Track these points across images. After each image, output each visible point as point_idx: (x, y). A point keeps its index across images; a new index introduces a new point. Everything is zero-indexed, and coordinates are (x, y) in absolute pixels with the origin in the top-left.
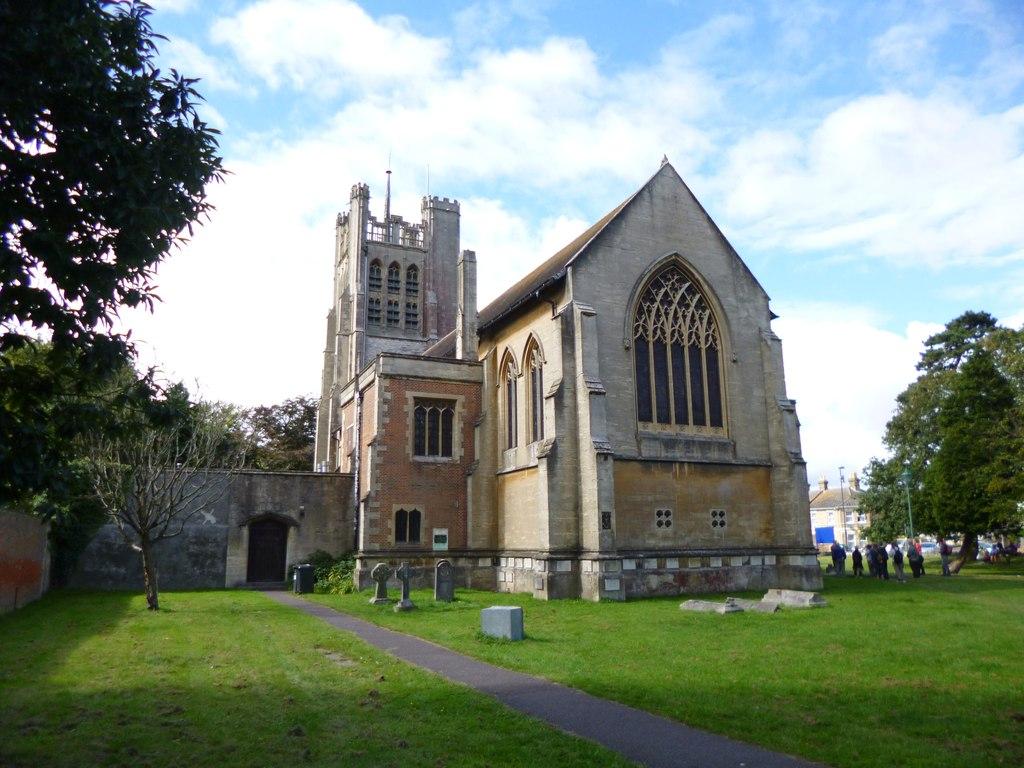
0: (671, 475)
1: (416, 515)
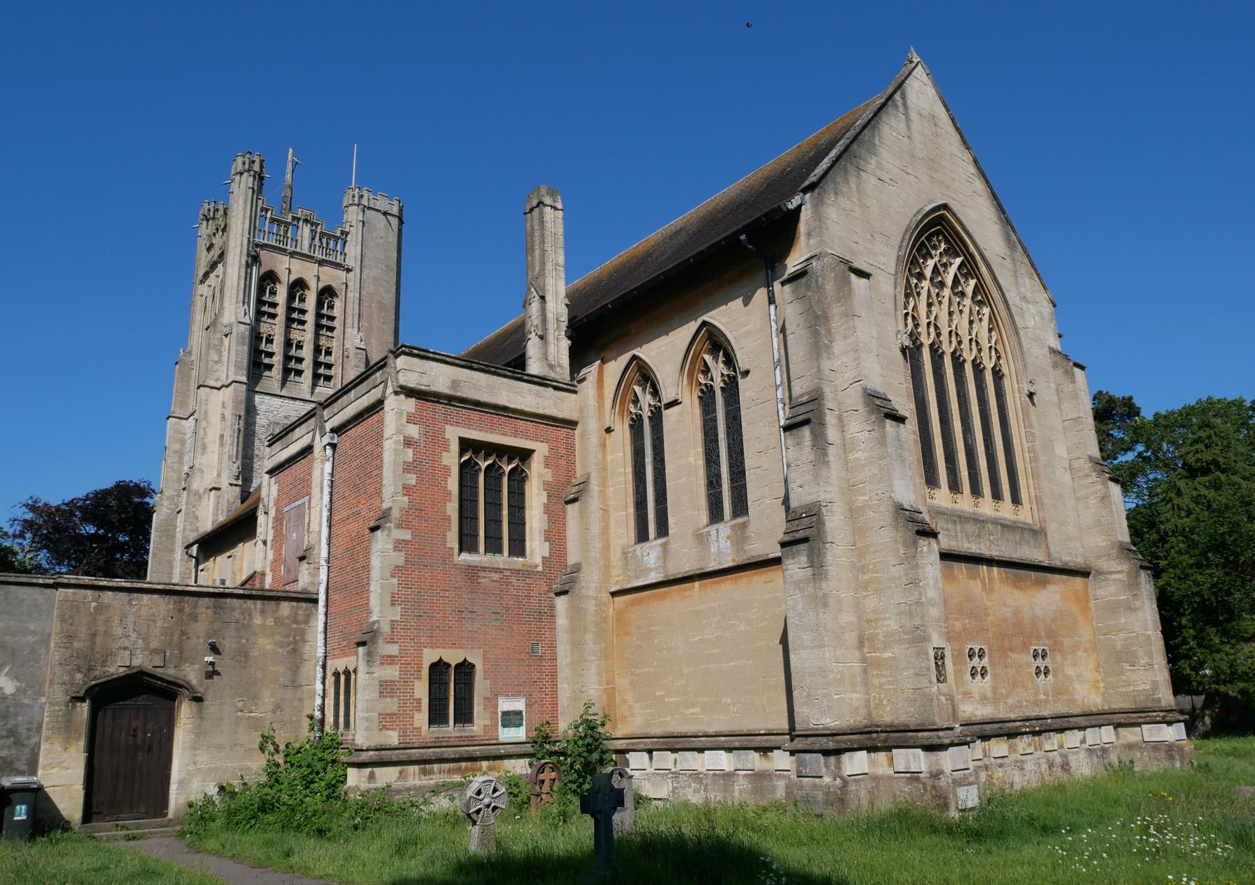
1: (465, 669)
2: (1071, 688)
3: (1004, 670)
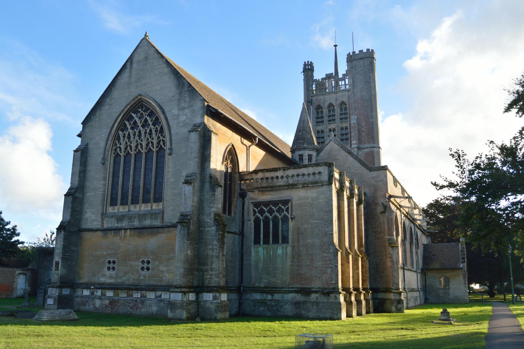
0: (118, 238)
2: (161, 275)
3: (124, 268)
